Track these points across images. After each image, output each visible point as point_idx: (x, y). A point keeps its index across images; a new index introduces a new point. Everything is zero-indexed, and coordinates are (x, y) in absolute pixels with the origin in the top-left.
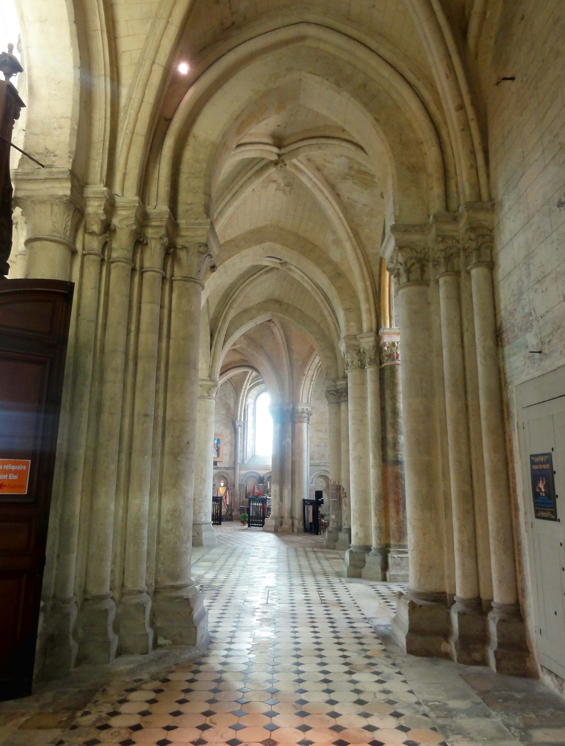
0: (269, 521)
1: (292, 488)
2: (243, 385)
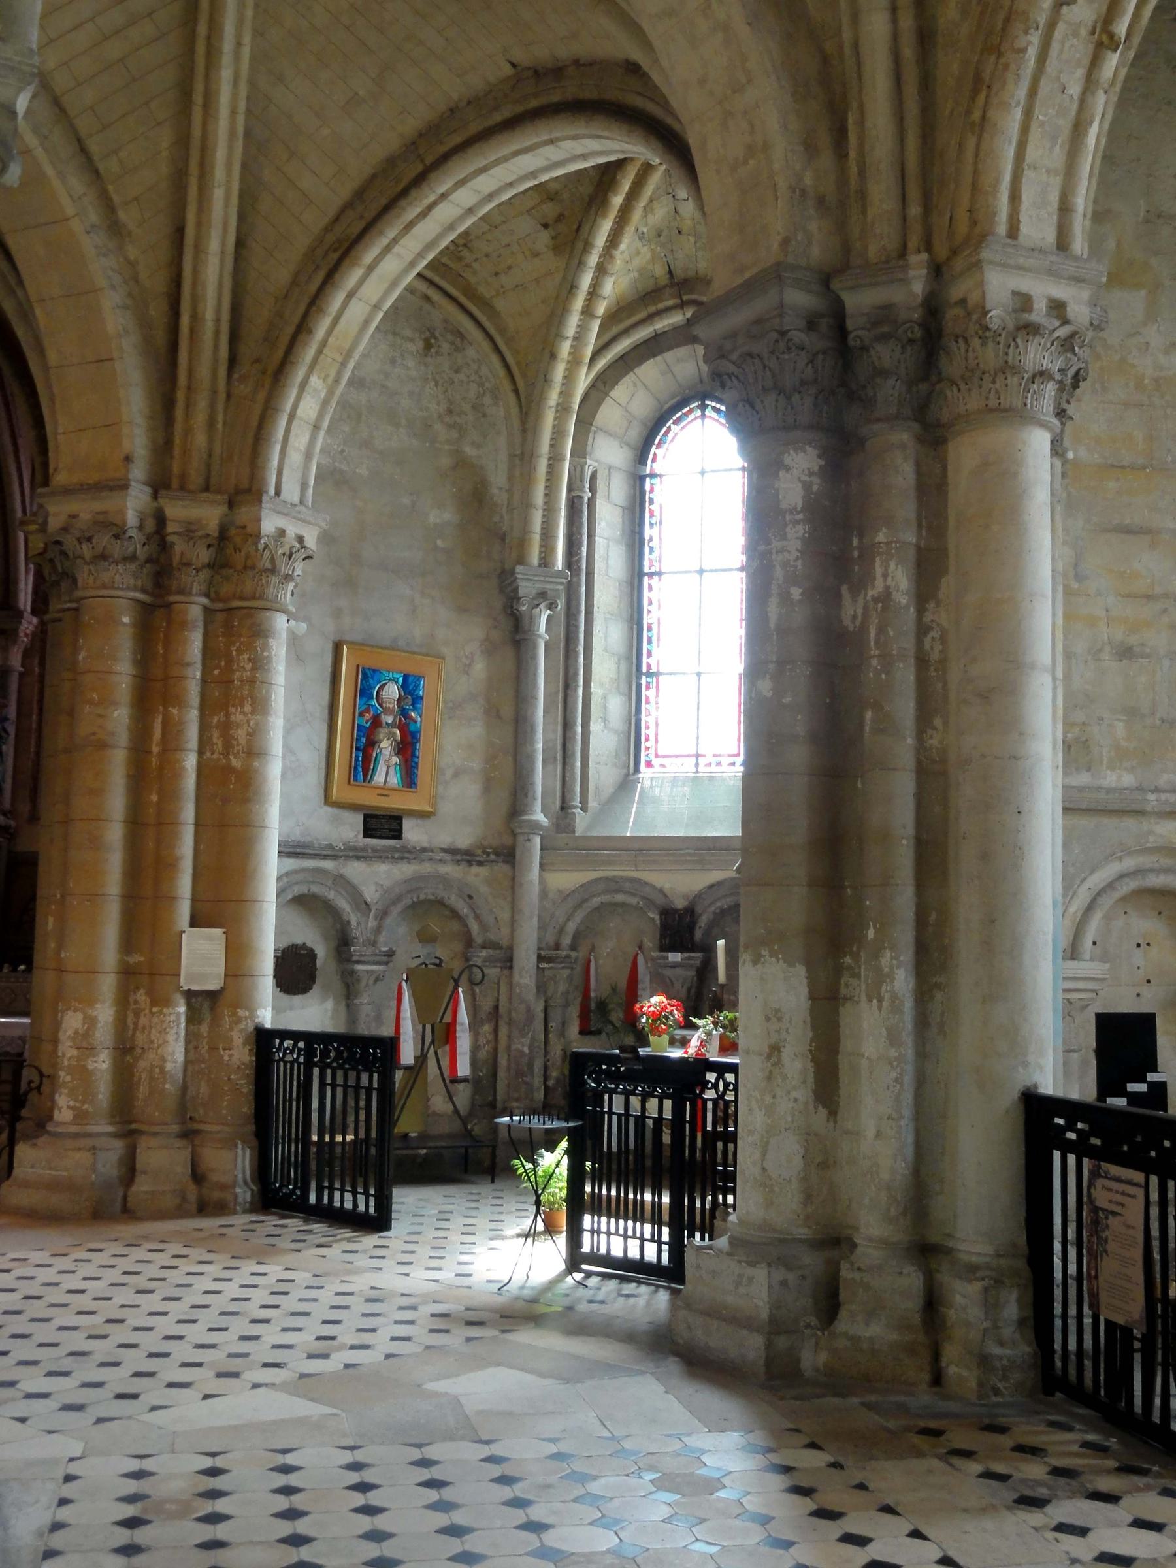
1: (924, 992)
2: (559, 336)
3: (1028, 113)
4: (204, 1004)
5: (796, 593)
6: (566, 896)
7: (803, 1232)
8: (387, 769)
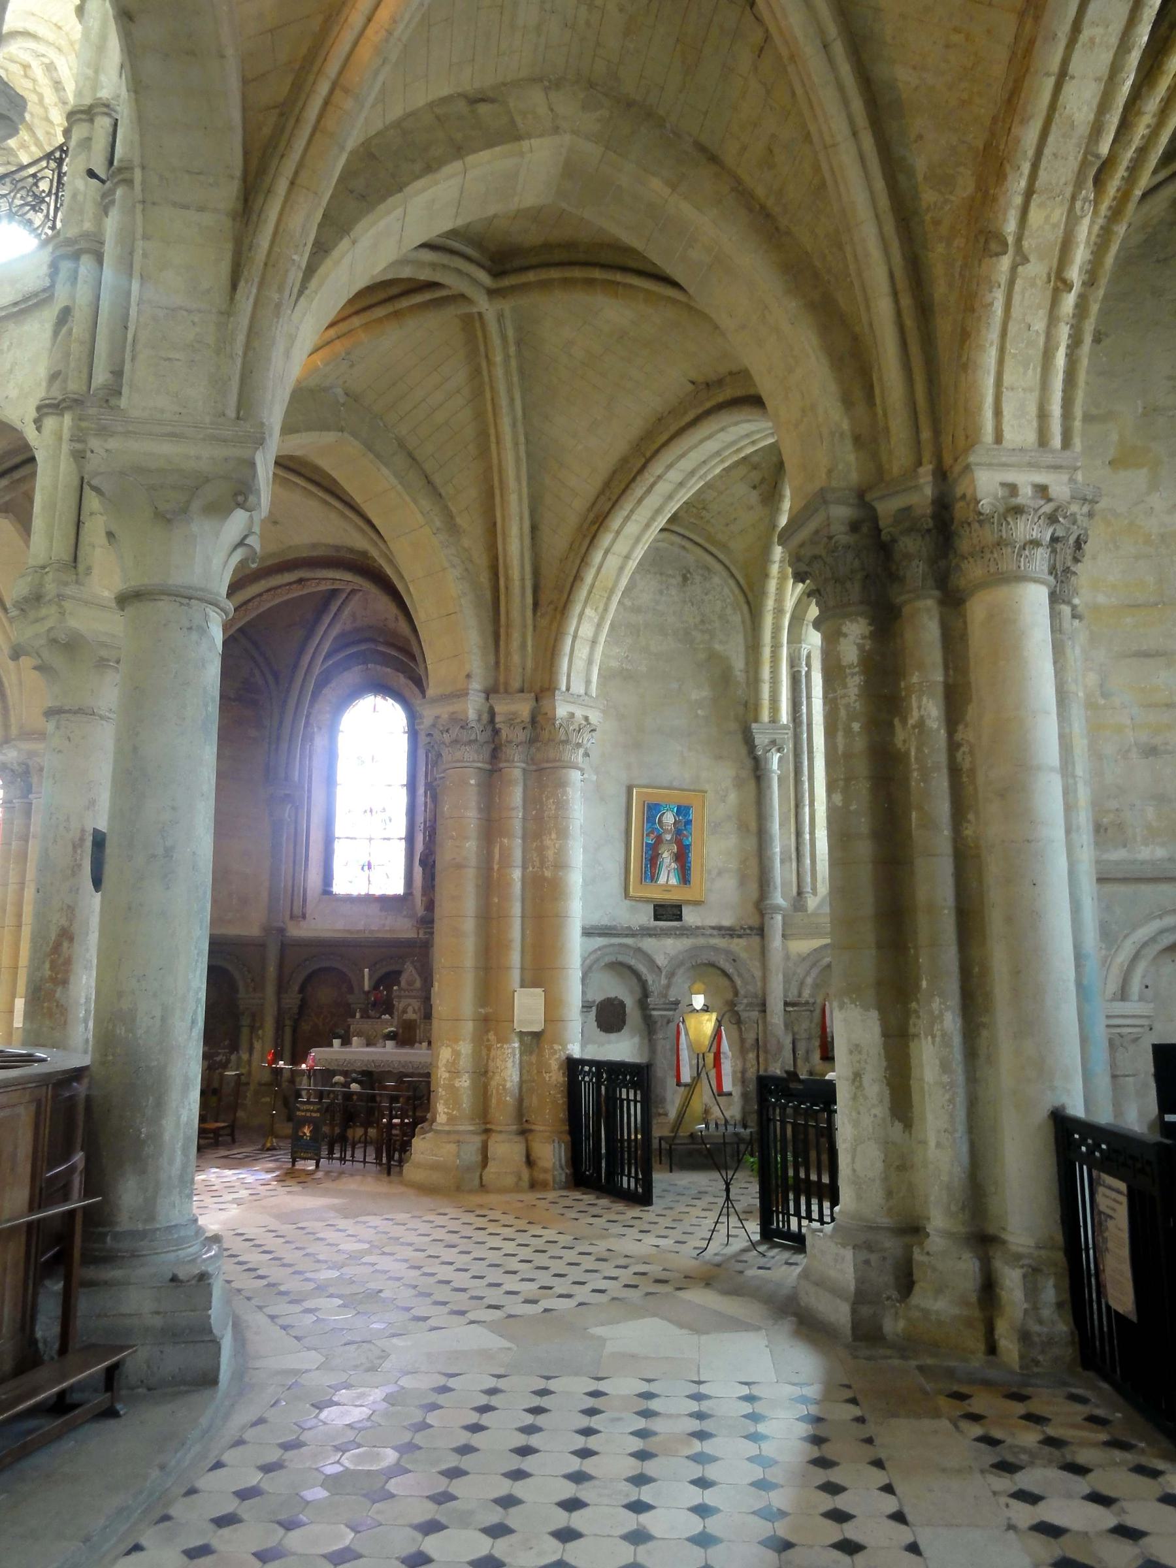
3: (1002, 350)
4: (534, 1041)
5: (856, 726)
7: (885, 1221)
8: (668, 875)
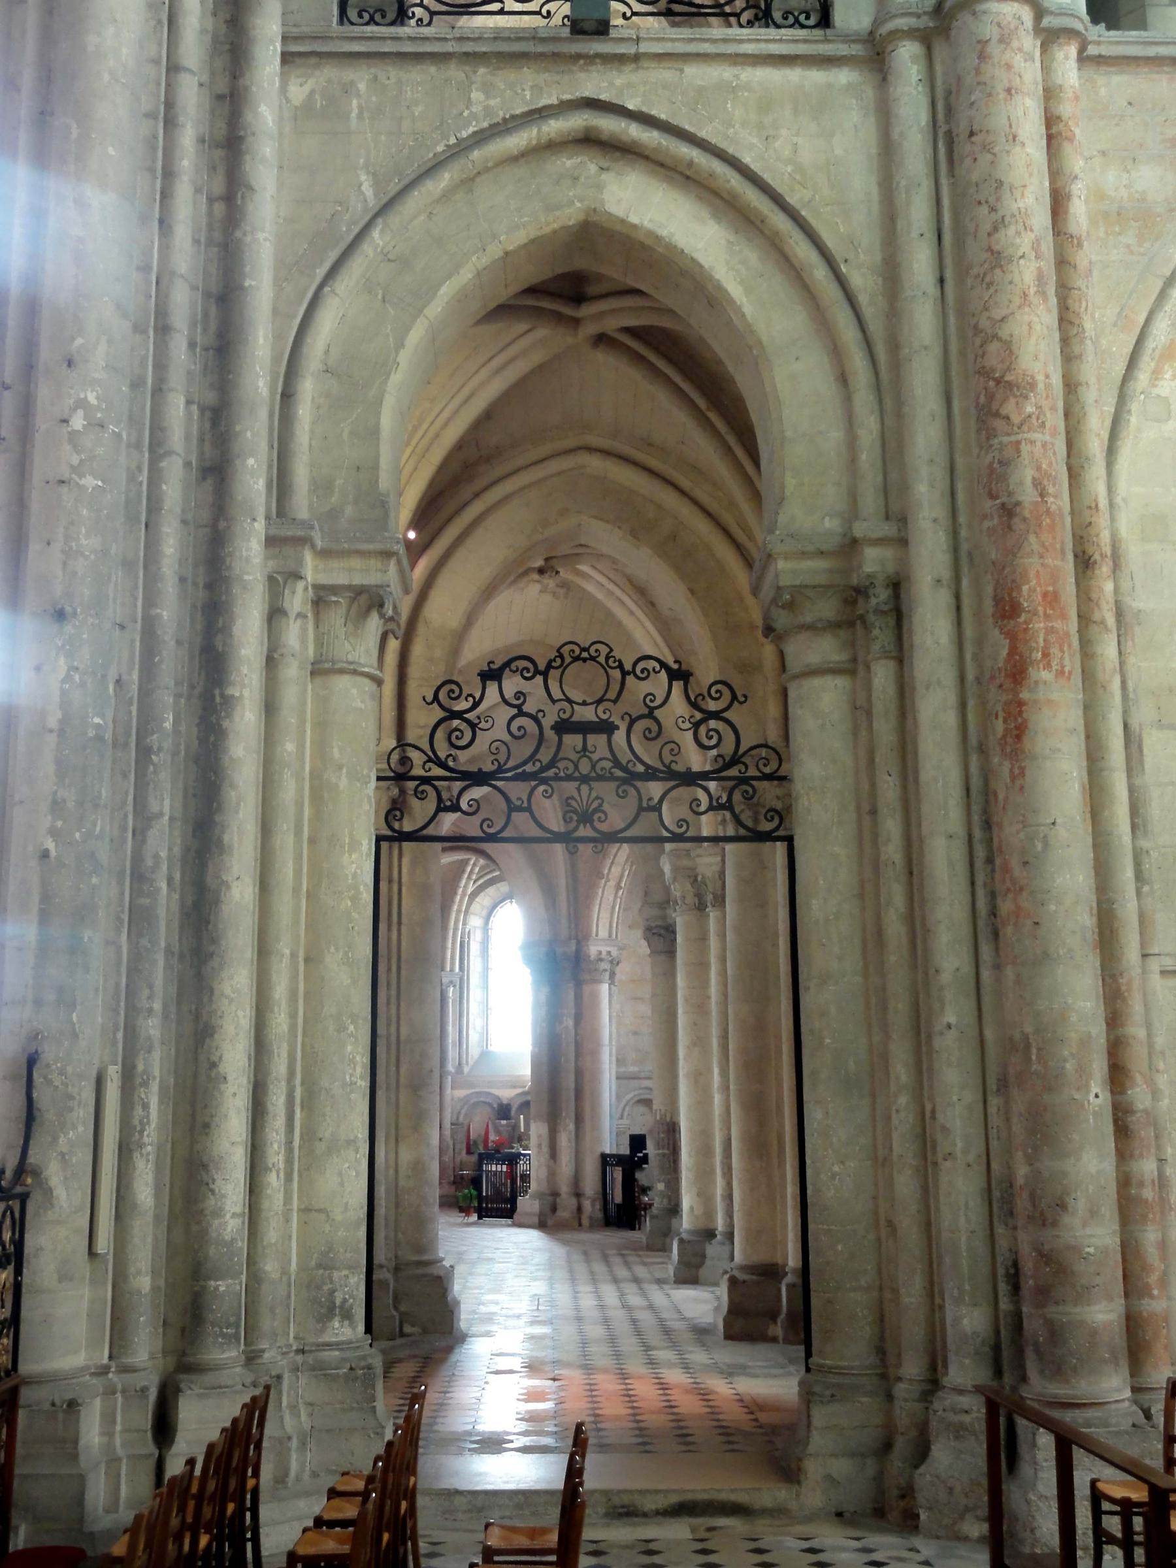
0: (526, 1204)
2: (458, 886)
6: (460, 1100)
